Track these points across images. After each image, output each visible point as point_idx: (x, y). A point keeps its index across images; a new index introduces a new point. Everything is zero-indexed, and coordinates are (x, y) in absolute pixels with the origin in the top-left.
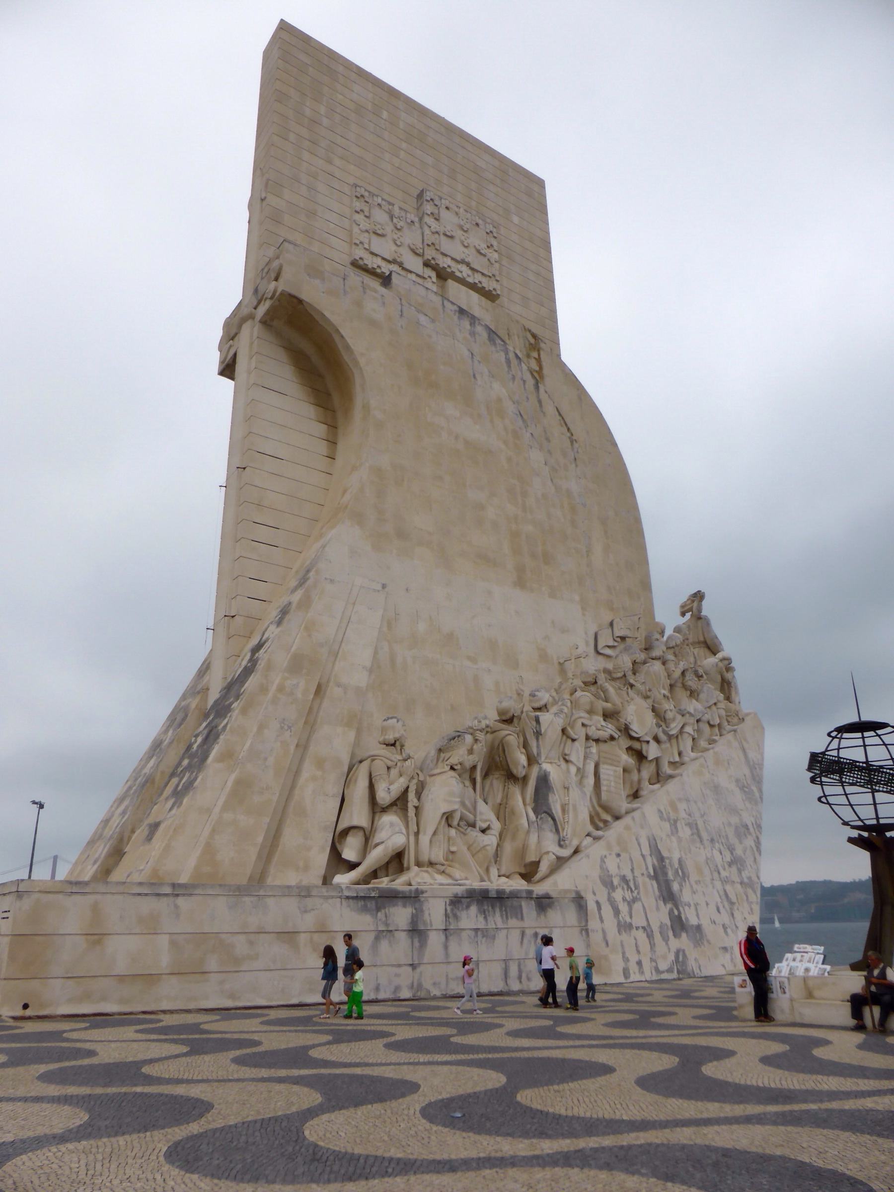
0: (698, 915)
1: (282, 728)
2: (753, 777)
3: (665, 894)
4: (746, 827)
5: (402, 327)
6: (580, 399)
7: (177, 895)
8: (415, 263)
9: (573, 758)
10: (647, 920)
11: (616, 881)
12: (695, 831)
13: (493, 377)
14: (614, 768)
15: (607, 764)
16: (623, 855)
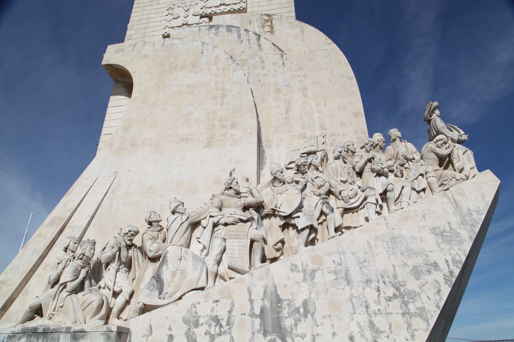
2: (464, 223)
3: (269, 328)
4: (435, 265)
12: (343, 275)
14: (240, 240)
15: (232, 238)
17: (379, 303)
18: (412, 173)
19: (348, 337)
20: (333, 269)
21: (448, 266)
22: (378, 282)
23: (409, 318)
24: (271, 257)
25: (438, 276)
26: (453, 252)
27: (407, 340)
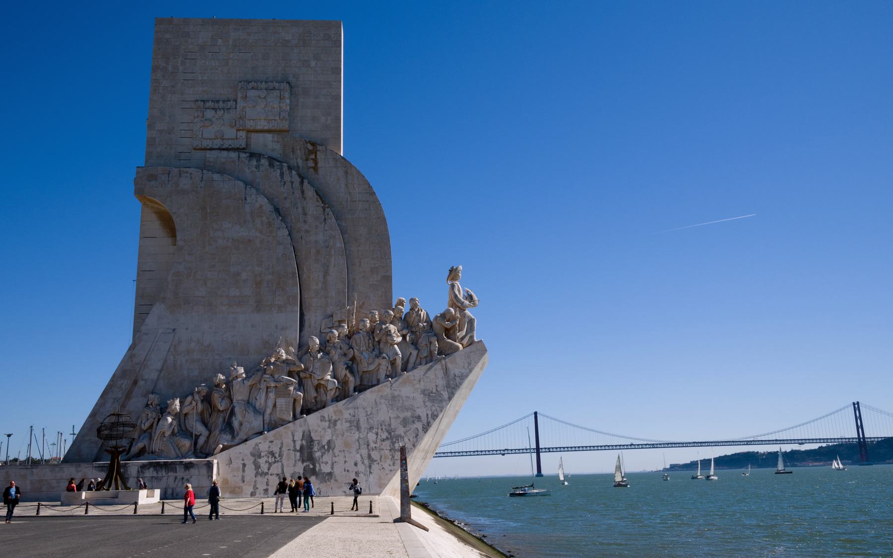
0: (332, 468)
1: (114, 402)
2: (448, 386)
3: (305, 458)
4: (419, 418)
5: (201, 187)
6: (346, 173)
7: (33, 468)
8: (230, 133)
9: (258, 398)
10: (283, 470)
11: (263, 454)
12: (355, 424)
13: (259, 194)
15: (280, 397)
16: (275, 441)
17: (376, 443)
18: (420, 340)
19: (353, 464)
20: (349, 419)
21: (428, 418)
22: (378, 429)
23: (393, 453)
24: (307, 408)
25: (419, 425)
26: (434, 408)
27: (390, 465)
